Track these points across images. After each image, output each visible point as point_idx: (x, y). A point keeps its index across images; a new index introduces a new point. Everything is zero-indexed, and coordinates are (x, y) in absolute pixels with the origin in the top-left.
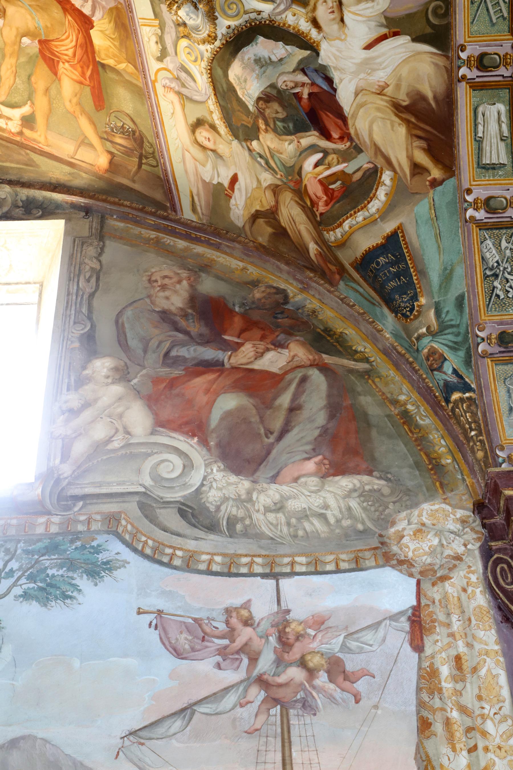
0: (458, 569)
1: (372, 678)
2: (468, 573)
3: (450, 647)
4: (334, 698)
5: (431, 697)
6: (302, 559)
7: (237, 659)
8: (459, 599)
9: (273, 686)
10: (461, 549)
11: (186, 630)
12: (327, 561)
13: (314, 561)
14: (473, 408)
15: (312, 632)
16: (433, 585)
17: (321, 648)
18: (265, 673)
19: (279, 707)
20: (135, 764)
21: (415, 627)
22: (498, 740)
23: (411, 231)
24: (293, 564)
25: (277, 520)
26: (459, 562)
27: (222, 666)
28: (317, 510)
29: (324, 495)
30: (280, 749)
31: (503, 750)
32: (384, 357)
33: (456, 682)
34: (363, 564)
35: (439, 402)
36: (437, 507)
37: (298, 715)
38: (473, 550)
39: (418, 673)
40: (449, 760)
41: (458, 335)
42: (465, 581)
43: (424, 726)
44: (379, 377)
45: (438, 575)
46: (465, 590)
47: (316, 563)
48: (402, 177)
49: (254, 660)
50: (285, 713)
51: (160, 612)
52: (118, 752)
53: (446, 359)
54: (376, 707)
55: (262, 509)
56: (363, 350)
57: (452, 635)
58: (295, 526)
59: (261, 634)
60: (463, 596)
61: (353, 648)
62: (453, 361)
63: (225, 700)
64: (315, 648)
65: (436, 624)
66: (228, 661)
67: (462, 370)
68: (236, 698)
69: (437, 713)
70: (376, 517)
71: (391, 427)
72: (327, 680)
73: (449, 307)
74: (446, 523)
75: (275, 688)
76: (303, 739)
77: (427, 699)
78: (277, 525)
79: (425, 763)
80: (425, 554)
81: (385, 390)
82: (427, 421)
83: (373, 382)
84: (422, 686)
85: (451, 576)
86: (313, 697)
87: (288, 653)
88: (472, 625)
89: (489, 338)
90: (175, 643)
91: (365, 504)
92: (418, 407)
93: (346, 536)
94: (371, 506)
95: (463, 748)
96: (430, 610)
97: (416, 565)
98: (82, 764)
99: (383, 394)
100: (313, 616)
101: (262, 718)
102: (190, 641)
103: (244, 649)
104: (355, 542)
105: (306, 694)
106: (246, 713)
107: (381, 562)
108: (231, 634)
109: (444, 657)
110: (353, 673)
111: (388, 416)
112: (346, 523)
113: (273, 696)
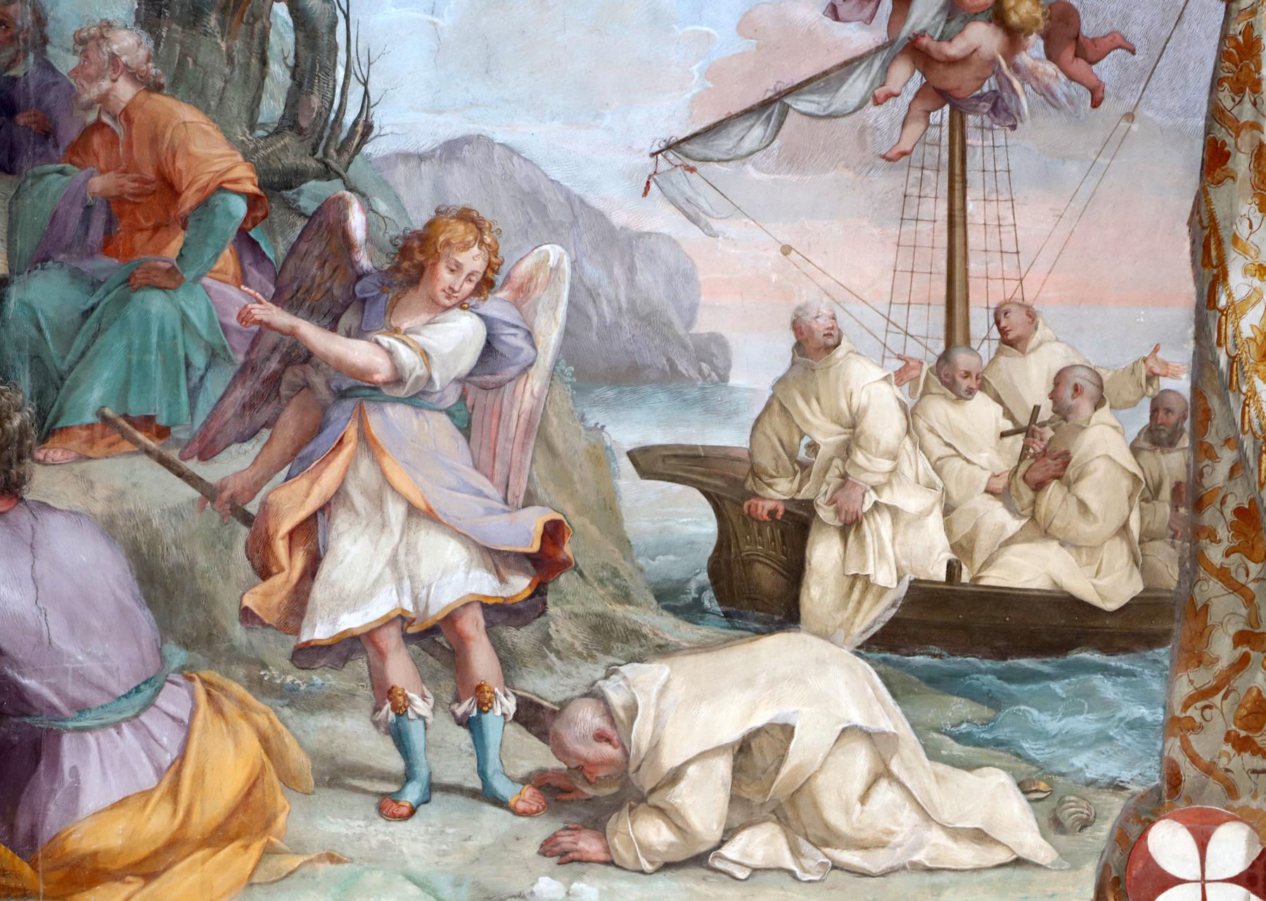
1: (1129, 54)
4: (1053, 95)
5: (1237, 99)
9: (939, 62)
18: (923, 33)
20: (680, 208)
27: (842, 11)
30: (946, 194)
37: (982, 128)
39: (1219, 45)
40: (1251, 227)
43: (1215, 159)
50: (957, 121)
52: (648, 183)
54: (1130, 117)
63: (845, 87)
68: (868, 84)
69: (1242, 133)
72: (1043, 56)
75: (941, 66)
76: (989, 177)
77: (1228, 104)
84: (1223, 74)
86: (1014, 91)
98: (582, 202)
101: (915, 129)
105: (999, 83)
110: (1093, 40)
113: (937, 85)
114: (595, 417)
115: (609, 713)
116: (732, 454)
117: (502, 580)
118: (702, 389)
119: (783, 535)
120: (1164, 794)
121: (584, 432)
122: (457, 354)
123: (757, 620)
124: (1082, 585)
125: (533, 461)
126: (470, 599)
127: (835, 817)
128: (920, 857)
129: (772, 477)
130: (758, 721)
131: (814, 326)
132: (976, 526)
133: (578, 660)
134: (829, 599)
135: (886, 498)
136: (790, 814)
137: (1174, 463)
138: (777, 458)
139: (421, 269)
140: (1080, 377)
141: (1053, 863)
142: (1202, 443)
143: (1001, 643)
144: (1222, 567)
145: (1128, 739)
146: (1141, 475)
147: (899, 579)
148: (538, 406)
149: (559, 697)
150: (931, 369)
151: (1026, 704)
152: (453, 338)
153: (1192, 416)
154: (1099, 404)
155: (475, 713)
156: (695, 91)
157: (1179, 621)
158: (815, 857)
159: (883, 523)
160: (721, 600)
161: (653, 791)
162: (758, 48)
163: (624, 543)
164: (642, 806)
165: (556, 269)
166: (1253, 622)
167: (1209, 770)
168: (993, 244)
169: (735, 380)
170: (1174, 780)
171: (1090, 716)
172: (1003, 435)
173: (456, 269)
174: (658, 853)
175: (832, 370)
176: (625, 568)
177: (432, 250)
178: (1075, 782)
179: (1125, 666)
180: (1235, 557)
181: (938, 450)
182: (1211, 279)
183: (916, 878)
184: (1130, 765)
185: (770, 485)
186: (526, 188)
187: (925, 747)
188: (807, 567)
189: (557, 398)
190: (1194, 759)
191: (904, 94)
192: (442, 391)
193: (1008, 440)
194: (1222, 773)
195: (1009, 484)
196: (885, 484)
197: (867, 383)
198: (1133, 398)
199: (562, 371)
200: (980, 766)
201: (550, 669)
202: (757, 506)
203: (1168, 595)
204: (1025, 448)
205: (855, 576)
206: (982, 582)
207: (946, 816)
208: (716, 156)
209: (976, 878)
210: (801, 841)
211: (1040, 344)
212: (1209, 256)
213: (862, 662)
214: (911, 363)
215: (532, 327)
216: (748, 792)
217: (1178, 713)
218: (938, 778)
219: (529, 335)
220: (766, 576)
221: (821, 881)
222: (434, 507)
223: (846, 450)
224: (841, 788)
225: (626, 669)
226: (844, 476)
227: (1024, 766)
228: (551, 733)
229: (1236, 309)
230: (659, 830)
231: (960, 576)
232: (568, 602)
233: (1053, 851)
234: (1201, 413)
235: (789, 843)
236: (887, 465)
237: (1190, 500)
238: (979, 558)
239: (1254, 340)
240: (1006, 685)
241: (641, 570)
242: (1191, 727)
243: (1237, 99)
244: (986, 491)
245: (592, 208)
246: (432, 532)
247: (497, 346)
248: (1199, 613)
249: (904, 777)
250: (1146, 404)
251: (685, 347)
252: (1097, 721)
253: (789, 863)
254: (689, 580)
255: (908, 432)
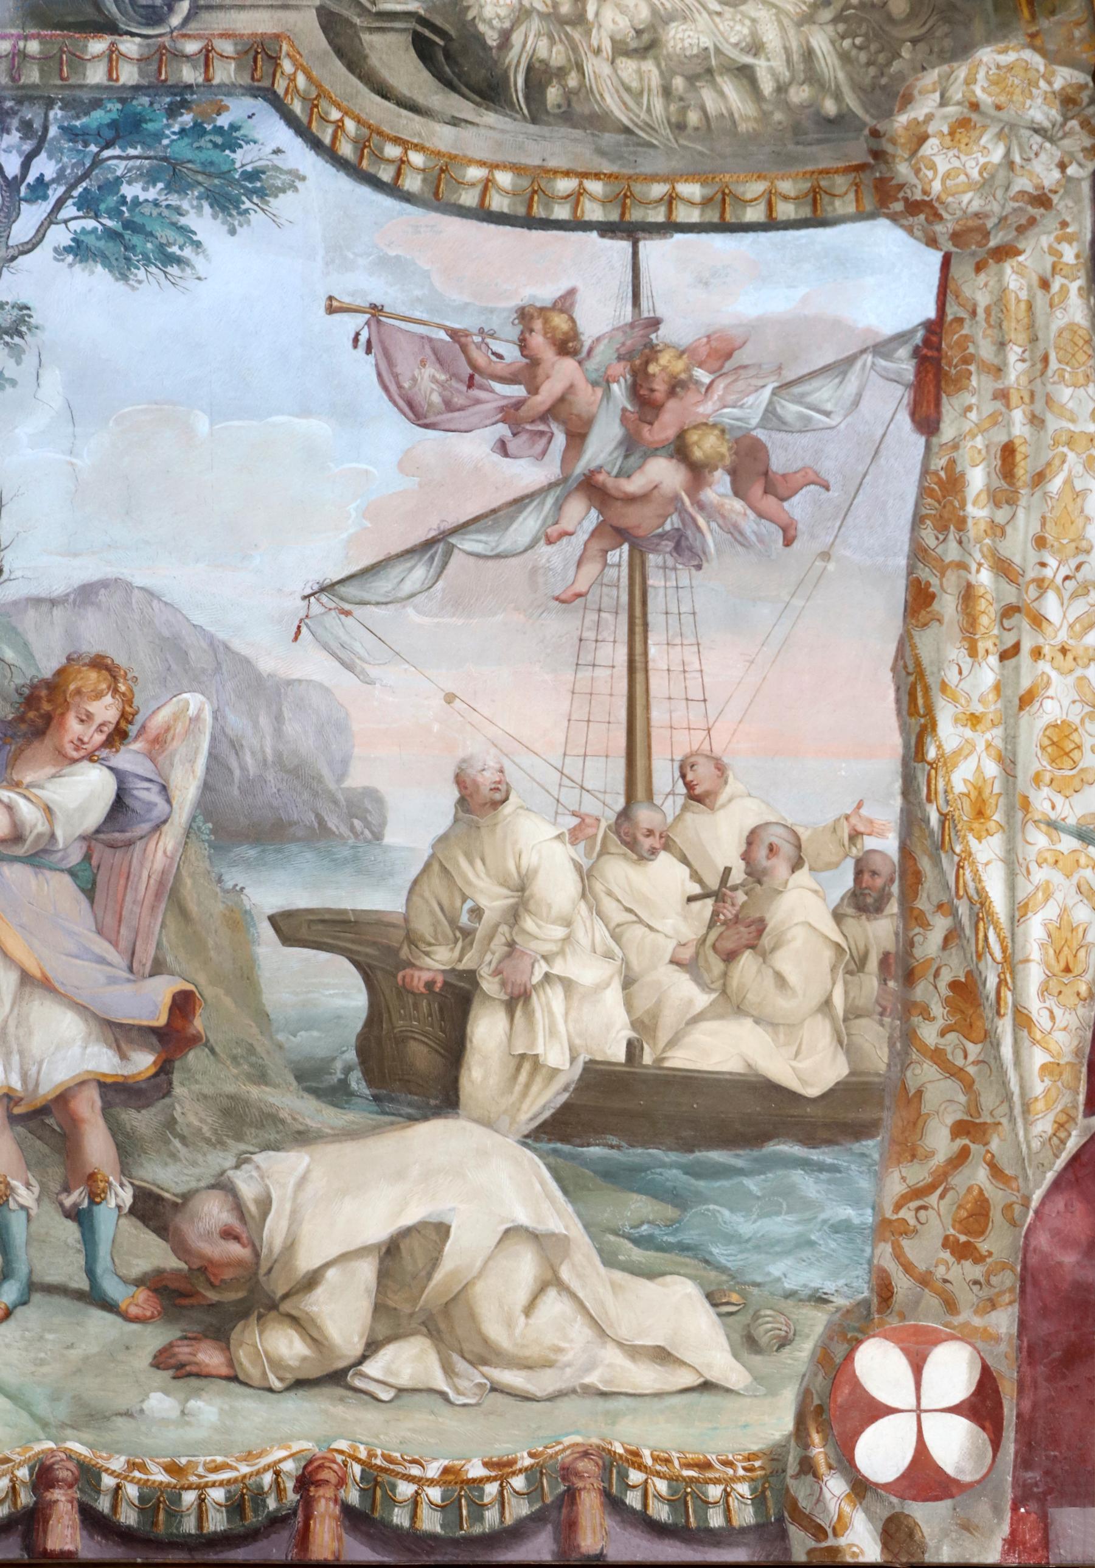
0: (1036, 230)
1: (822, 490)
2: (1059, 240)
3: (995, 424)
4: (741, 533)
5: (941, 537)
6: (692, 190)
7: (542, 433)
8: (1030, 306)
9: (617, 499)
10: (1051, 177)
11: (433, 358)
12: (749, 196)
13: (719, 196)
15: (703, 376)
16: (979, 268)
17: (721, 415)
18: (599, 470)
19: (626, 547)
21: (927, 372)
22: (1063, 636)
24: (670, 200)
25: (641, 79)
26: (1042, 210)
27: (511, 447)
28: (734, 54)
29: (753, 14)
30: (625, 638)
31: (1070, 656)
33: (997, 505)
34: (829, 209)
36: (1011, 57)
37: (665, 568)
38: (1079, 180)
40: (960, 673)
42: (1049, 260)
43: (919, 601)
45: (992, 244)
46: (1045, 284)
47: (724, 200)
49: (578, 436)
50: (638, 561)
51: (376, 310)
52: (299, 627)
54: (826, 556)
55: (607, 45)
57: (1002, 395)
58: (681, 99)
59: (594, 376)
60: (1041, 300)
61: (789, 418)
63: (515, 526)
64: (709, 416)
65: (972, 368)
66: (524, 437)
68: (539, 522)
69: (949, 573)
70: (868, 81)
72: (730, 492)
74: (1028, 102)
75: (619, 504)
76: (673, 620)
77: (931, 542)
78: (641, 93)
79: (912, 678)
80: (971, 186)
84: (924, 512)
85: (1020, 246)
86: (698, 528)
87: (651, 424)
88: (1050, 372)
90: (410, 388)
91: (847, 43)
93: (797, 130)
94: (860, 48)
95: (991, 648)
96: (964, 332)
97: (945, 215)
98: (227, 647)
100: (708, 337)
101: (591, 570)
102: (442, 385)
103: (559, 410)
104: (814, 149)
105: (683, 521)
106: (556, 558)
107: (868, 206)
108: (529, 373)
109: (980, 446)
110: (784, 476)
112: (800, 94)
113: (615, 523)
114: (234, 877)
115: (239, 1207)
116: (385, 919)
117: (123, 1057)
118: (353, 847)
119: (441, 1010)
120: (874, 1308)
121: (220, 894)
122: (83, 810)
123: (410, 1104)
124: (779, 1067)
125: (163, 925)
126: (85, 1077)
127: (495, 1331)
128: (593, 1379)
129: (430, 944)
130: (410, 1217)
131: (480, 779)
132: (659, 1004)
133: (205, 1147)
134: (493, 1081)
135: (558, 969)
136: (442, 1326)
137: (881, 932)
138: (436, 924)
139: (48, 718)
140: (776, 836)
141: (746, 1389)
142: (912, 909)
143: (687, 1133)
144: (937, 1049)
145: (833, 1245)
146: (844, 945)
147: (573, 1060)
148: (171, 865)
149: (182, 1189)
150: (609, 827)
151: (716, 1203)
152: (80, 793)
153: (901, 878)
154: (797, 865)
155: (85, 1204)
156: (352, 531)
157: (889, 1109)
158: (471, 1377)
159: (555, 997)
160: (370, 1083)
161: (286, 1296)
162: (420, 485)
163: (262, 1017)
164: (273, 1314)
165: (197, 719)
166: (973, 1111)
167: (924, 1280)
168: (677, 692)
169: (389, 839)
170: (885, 1292)
171: (789, 1218)
172: (691, 899)
173: (86, 719)
174: (288, 1368)
175: (499, 830)
176: (262, 1045)
177: (61, 700)
178: (772, 1294)
179: (829, 1160)
180: (952, 1037)
181: (617, 915)
182: (918, 729)
183: (588, 1403)
184: (834, 1275)
185: (427, 954)
186: (166, 633)
187: (600, 1251)
188: (468, 1046)
189: (193, 858)
190: (908, 1268)
191: (579, 533)
192: (65, 849)
193: (696, 905)
194: (940, 1284)
195: (697, 954)
196: (557, 953)
197: (537, 841)
198: (834, 859)
199: (199, 828)
200: (663, 1274)
201: (173, 1156)
202: (412, 976)
203: (876, 1079)
204: (715, 914)
205: (523, 1057)
206: (667, 1064)
207: (624, 1332)
208: (374, 598)
209: (657, 1404)
210: (456, 1358)
211: (730, 800)
212: (916, 705)
213: (528, 1152)
214: (587, 820)
215: (167, 780)
216: (394, 1300)
217: (889, 1214)
218: (615, 1287)
219: (164, 789)
220: (421, 1056)
221: (477, 1405)
222: (50, 975)
223: (514, 915)
224: (501, 1295)
225: (259, 1158)
226: (511, 945)
227: (713, 1274)
228: (171, 1228)
229: (946, 762)
230: (291, 1342)
231: (641, 1056)
232: (197, 1082)
233: (747, 1373)
234: (910, 875)
235: (441, 1360)
236: (559, 932)
237: (900, 973)
238: (663, 1037)
239: (968, 795)
240: (693, 1181)
241: (281, 1047)
242: (903, 1230)
243: (941, 537)
244: (672, 962)
245: (238, 654)
246: (47, 1003)
247: (128, 801)
248: (911, 1100)
249: (575, 1285)
250: (849, 866)
251: (336, 802)
252: (797, 1223)
253: (440, 1382)
254: (334, 1059)
255: (583, 896)
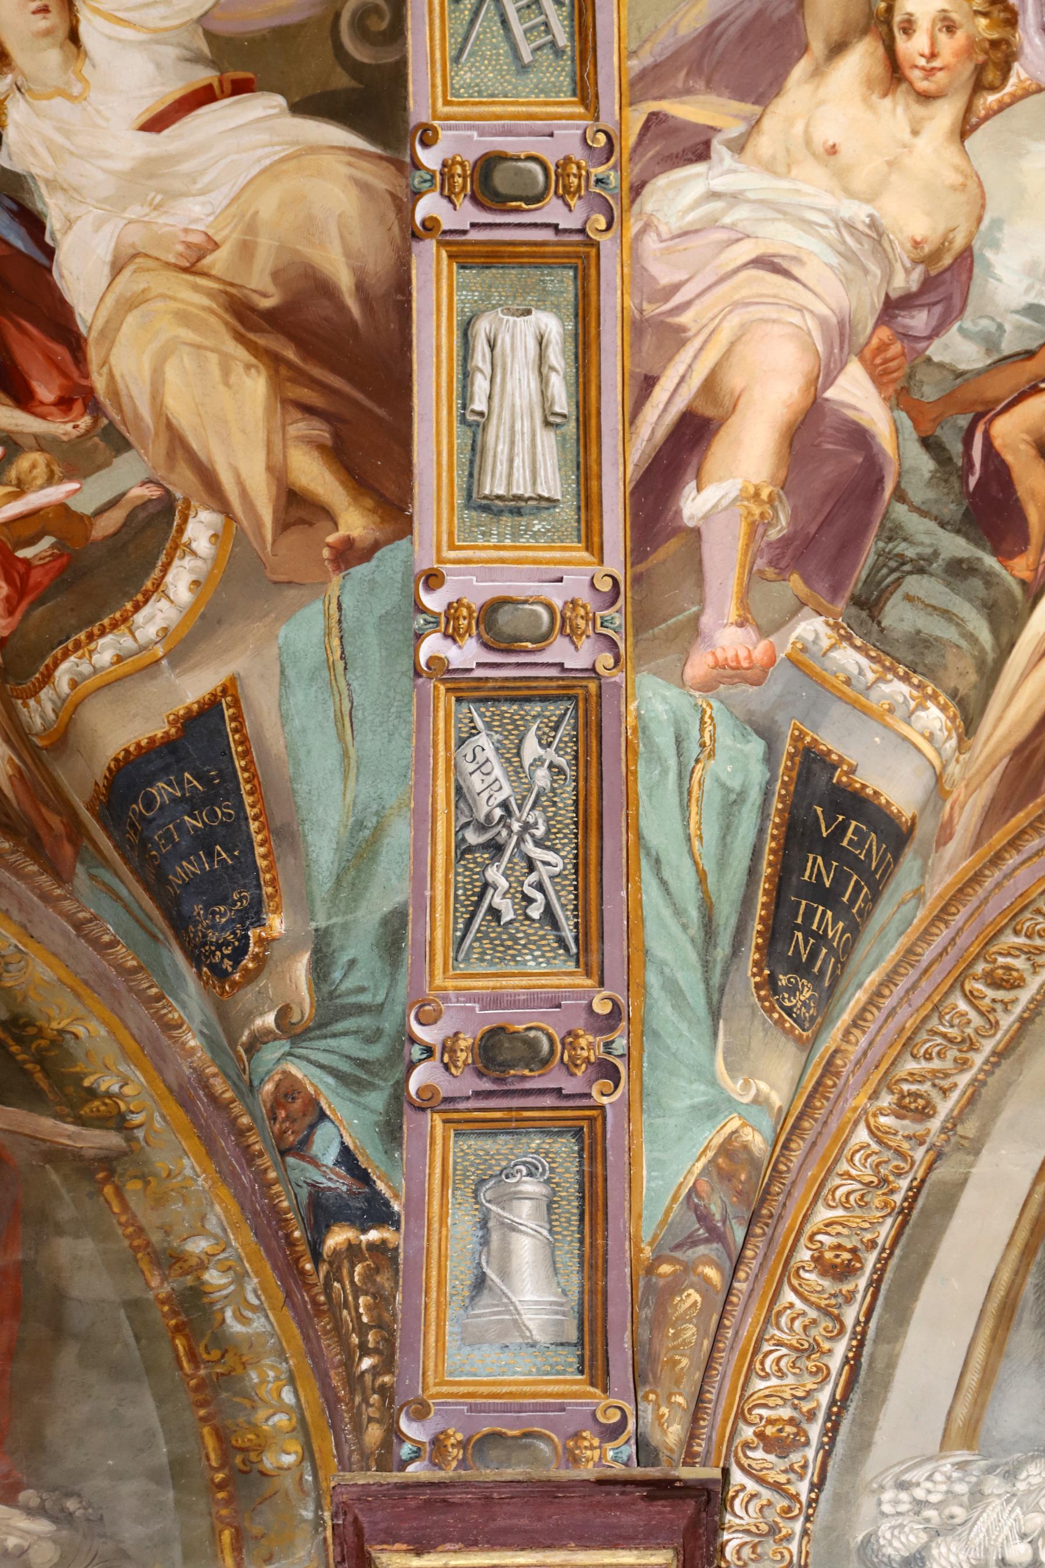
14: (383, 1279)
23: (262, 702)
32: (180, 1112)
35: (297, 1260)
41: (373, 1037)
44: (143, 1178)
48: (249, 532)
53: (323, 1116)
56: (115, 1088)
62: (348, 1121)
67: (371, 1156)
71: (132, 1341)
73: (359, 947)
81: (147, 1218)
82: (259, 1324)
83: (119, 1192)
89: (449, 1047)
92: (240, 1278)
99: (140, 1230)
111: (134, 1306)
